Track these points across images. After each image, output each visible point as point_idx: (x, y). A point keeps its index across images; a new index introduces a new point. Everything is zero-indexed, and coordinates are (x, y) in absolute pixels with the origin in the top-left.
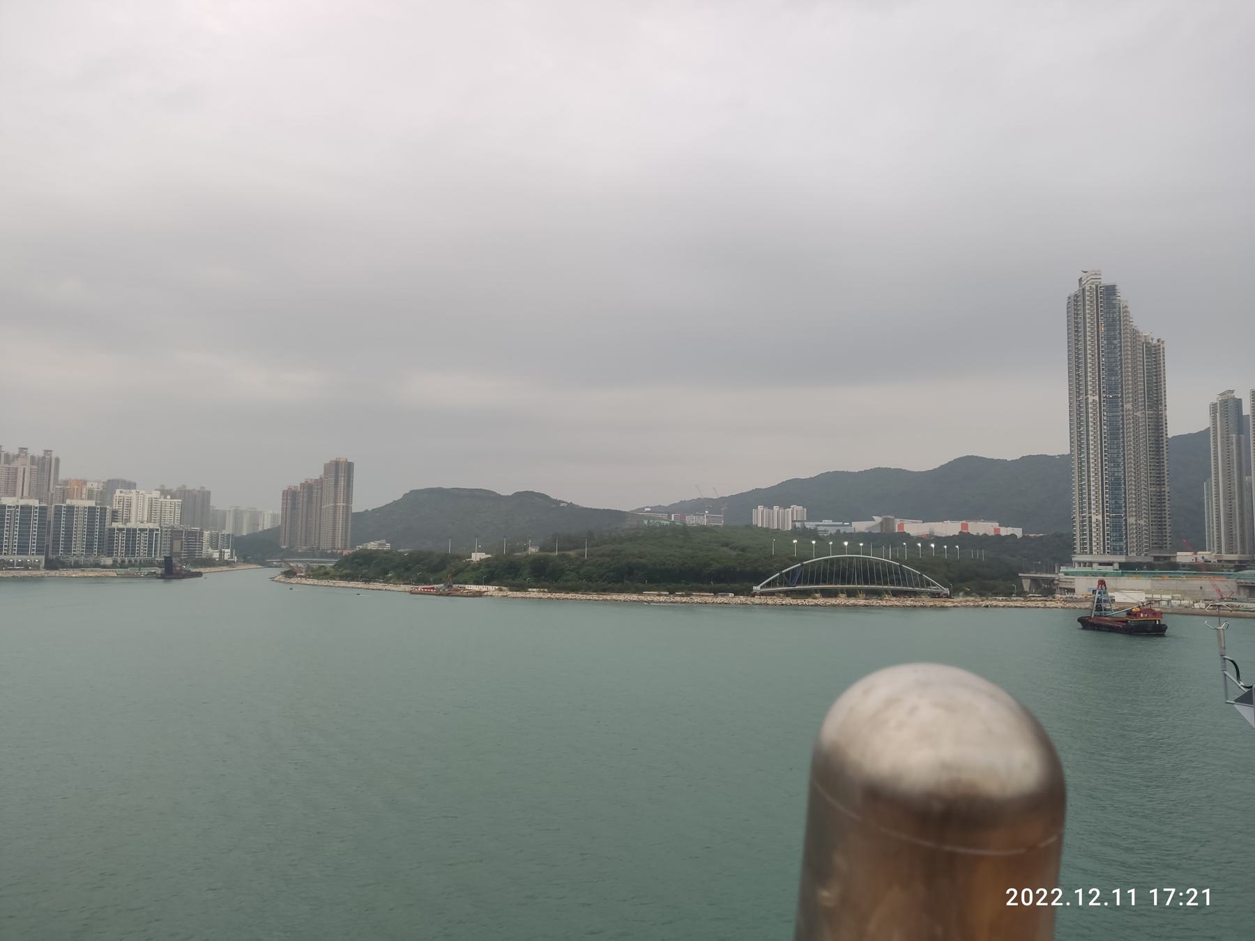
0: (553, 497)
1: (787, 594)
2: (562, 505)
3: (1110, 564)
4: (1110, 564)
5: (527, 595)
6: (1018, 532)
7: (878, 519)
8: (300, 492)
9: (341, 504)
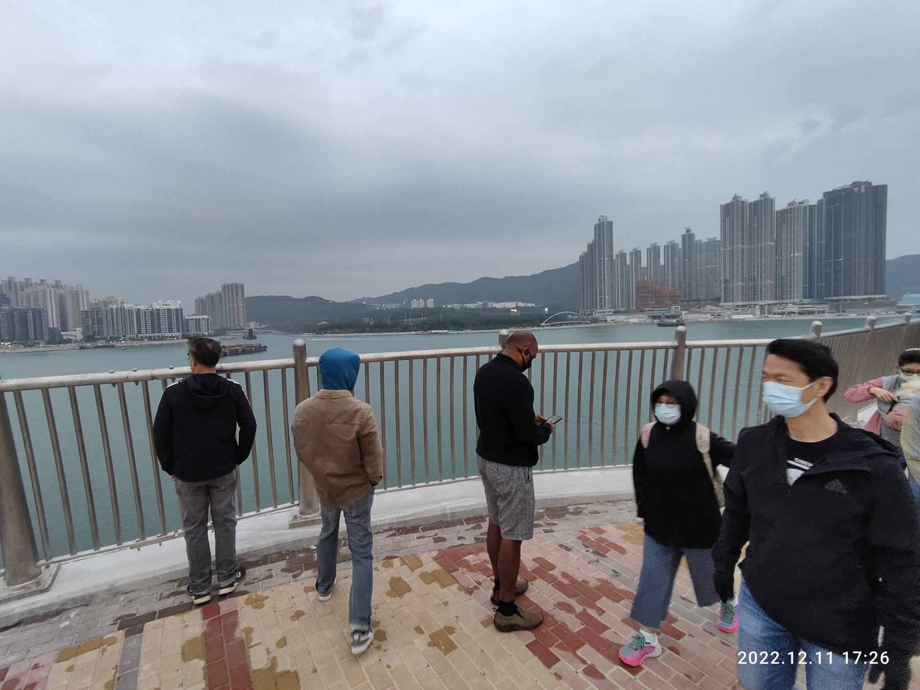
0: (325, 298)
1: (552, 325)
2: (330, 302)
3: (610, 312)
4: (610, 312)
5: (535, 329)
6: (533, 305)
7: (480, 303)
8: (205, 300)
9: (241, 305)
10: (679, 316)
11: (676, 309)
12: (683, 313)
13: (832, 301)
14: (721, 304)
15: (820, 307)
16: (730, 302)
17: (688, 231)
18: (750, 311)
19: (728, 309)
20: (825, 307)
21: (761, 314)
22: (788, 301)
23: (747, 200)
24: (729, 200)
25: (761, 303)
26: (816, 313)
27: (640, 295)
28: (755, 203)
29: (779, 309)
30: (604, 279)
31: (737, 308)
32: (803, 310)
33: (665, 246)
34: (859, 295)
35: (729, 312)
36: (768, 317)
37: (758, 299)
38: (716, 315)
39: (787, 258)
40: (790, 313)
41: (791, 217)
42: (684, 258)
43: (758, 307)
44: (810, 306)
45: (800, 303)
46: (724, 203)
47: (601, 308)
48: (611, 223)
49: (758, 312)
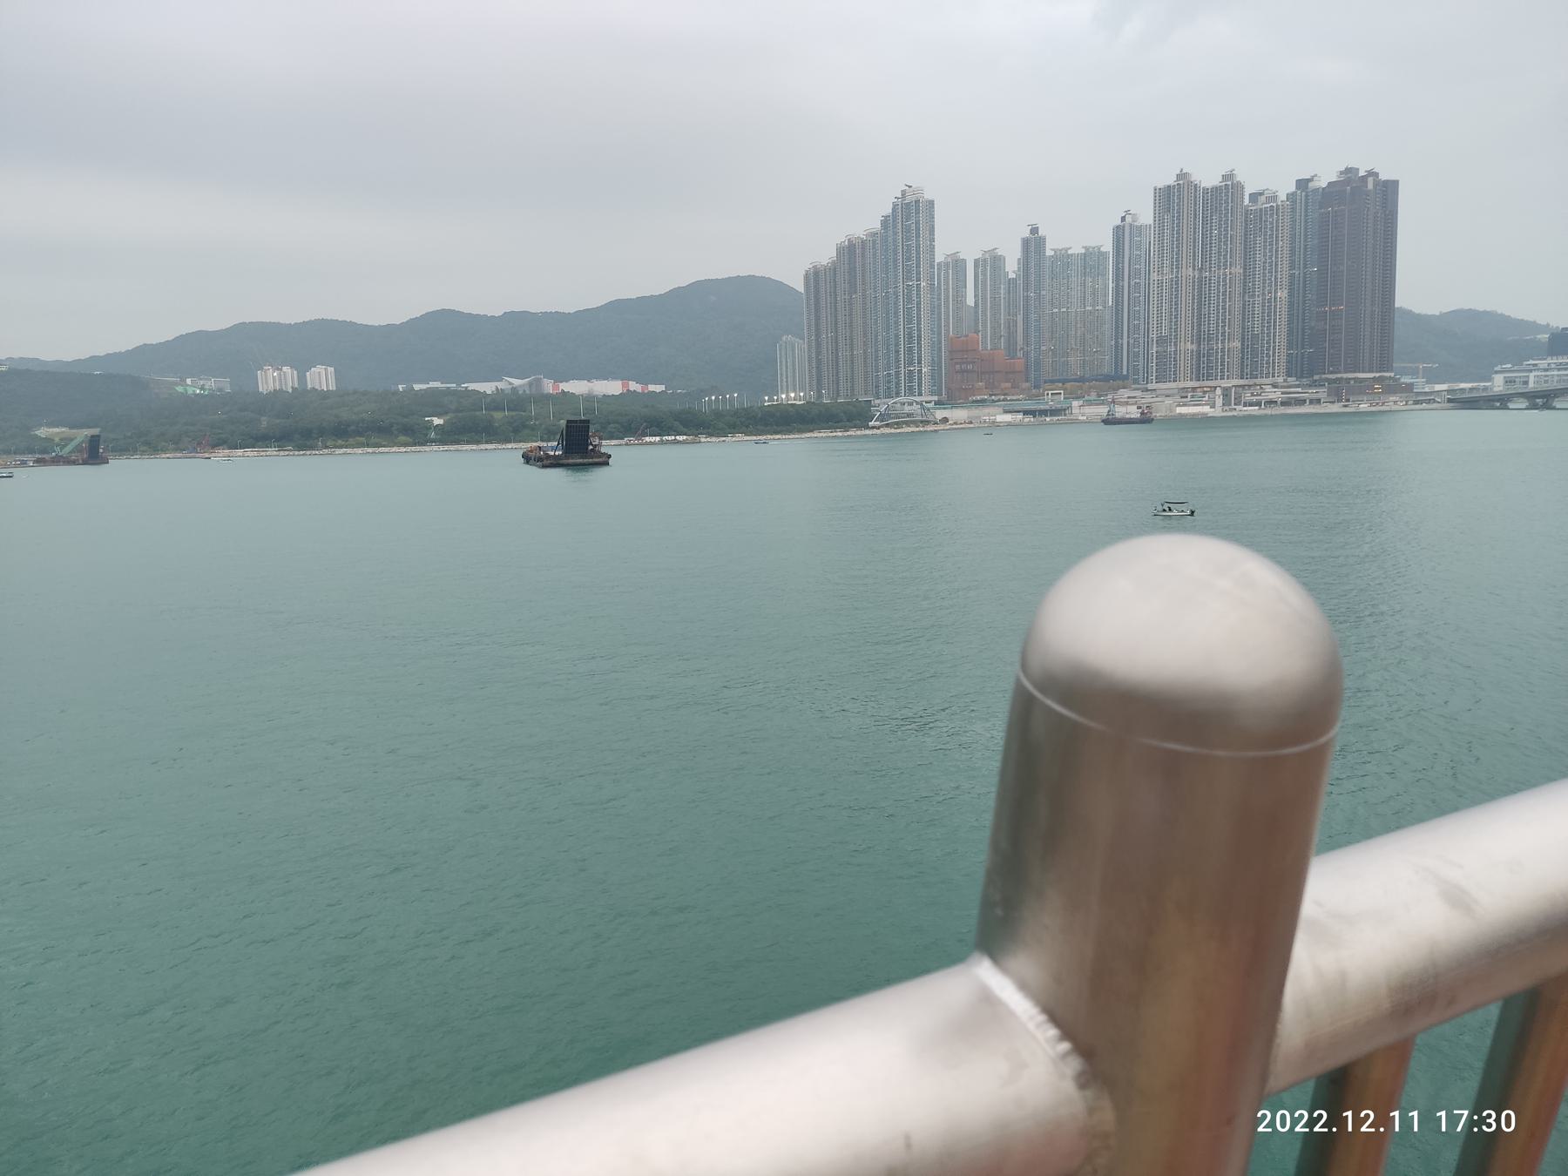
10: (1065, 410)
11: (1056, 397)
12: (1075, 403)
13: (1330, 381)
14: (1150, 386)
15: (1312, 393)
16: (1170, 381)
17: (1034, 230)
18: (1207, 398)
20: (1322, 393)
21: (1223, 405)
22: (1264, 381)
23: (1200, 182)
24: (1171, 180)
25: (1226, 383)
26: (1308, 401)
27: (958, 367)
28: (1216, 189)
29: (1252, 395)
30: (919, 330)
31: (1184, 395)
32: (1289, 398)
33: (976, 262)
35: (1168, 401)
37: (1217, 376)
39: (1264, 299)
40: (1271, 402)
41: (1272, 223)
43: (1219, 391)
44: (1300, 390)
45: (1285, 384)
46: (1160, 185)
47: (910, 391)
48: (931, 203)
49: (1219, 402)
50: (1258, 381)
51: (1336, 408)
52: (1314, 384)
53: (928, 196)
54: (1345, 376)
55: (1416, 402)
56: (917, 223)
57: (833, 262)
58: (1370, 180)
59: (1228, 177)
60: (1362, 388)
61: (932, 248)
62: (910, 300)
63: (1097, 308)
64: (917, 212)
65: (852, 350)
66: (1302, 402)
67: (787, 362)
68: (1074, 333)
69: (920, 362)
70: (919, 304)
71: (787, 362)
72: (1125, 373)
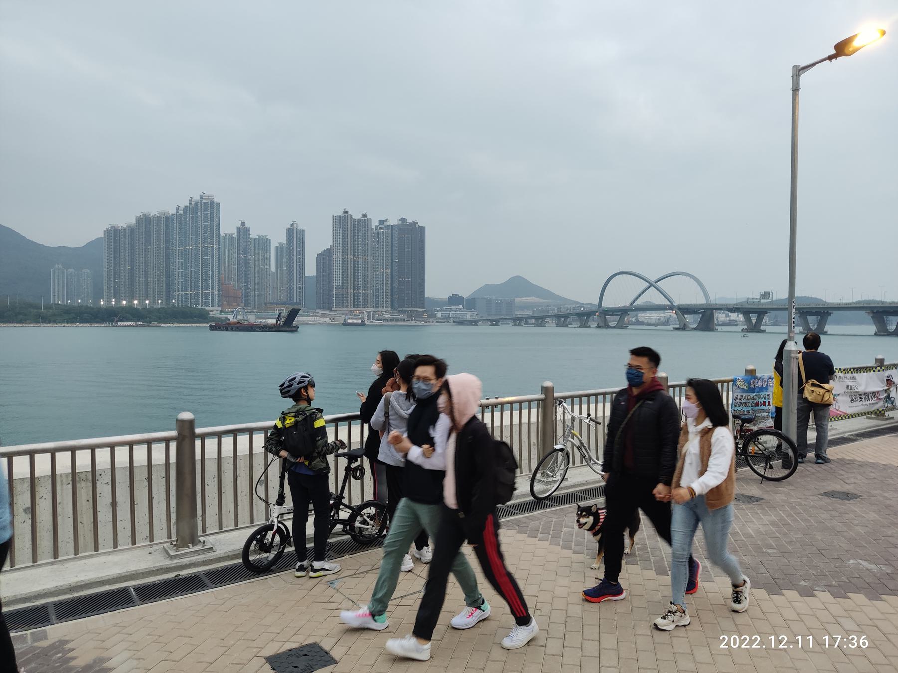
13: (408, 311)
15: (401, 316)
17: (243, 224)
19: (343, 314)
20: (405, 316)
22: (384, 309)
24: (340, 213)
28: (360, 221)
30: (213, 272)
34: (419, 308)
36: (372, 322)
37: (363, 306)
38: (332, 318)
40: (386, 319)
42: (239, 253)
43: (365, 313)
44: (397, 314)
50: (379, 309)
51: (413, 323)
52: (400, 312)
53: (216, 200)
54: (413, 309)
55: (437, 322)
56: (212, 214)
57: (129, 226)
58: (417, 226)
59: (365, 216)
60: (419, 315)
61: (219, 229)
62: (206, 254)
63: (266, 267)
64: (212, 207)
65: (146, 277)
66: (397, 320)
67: (58, 281)
68: (253, 279)
69: (212, 288)
70: (212, 257)
71: (58, 281)
72: (295, 301)
